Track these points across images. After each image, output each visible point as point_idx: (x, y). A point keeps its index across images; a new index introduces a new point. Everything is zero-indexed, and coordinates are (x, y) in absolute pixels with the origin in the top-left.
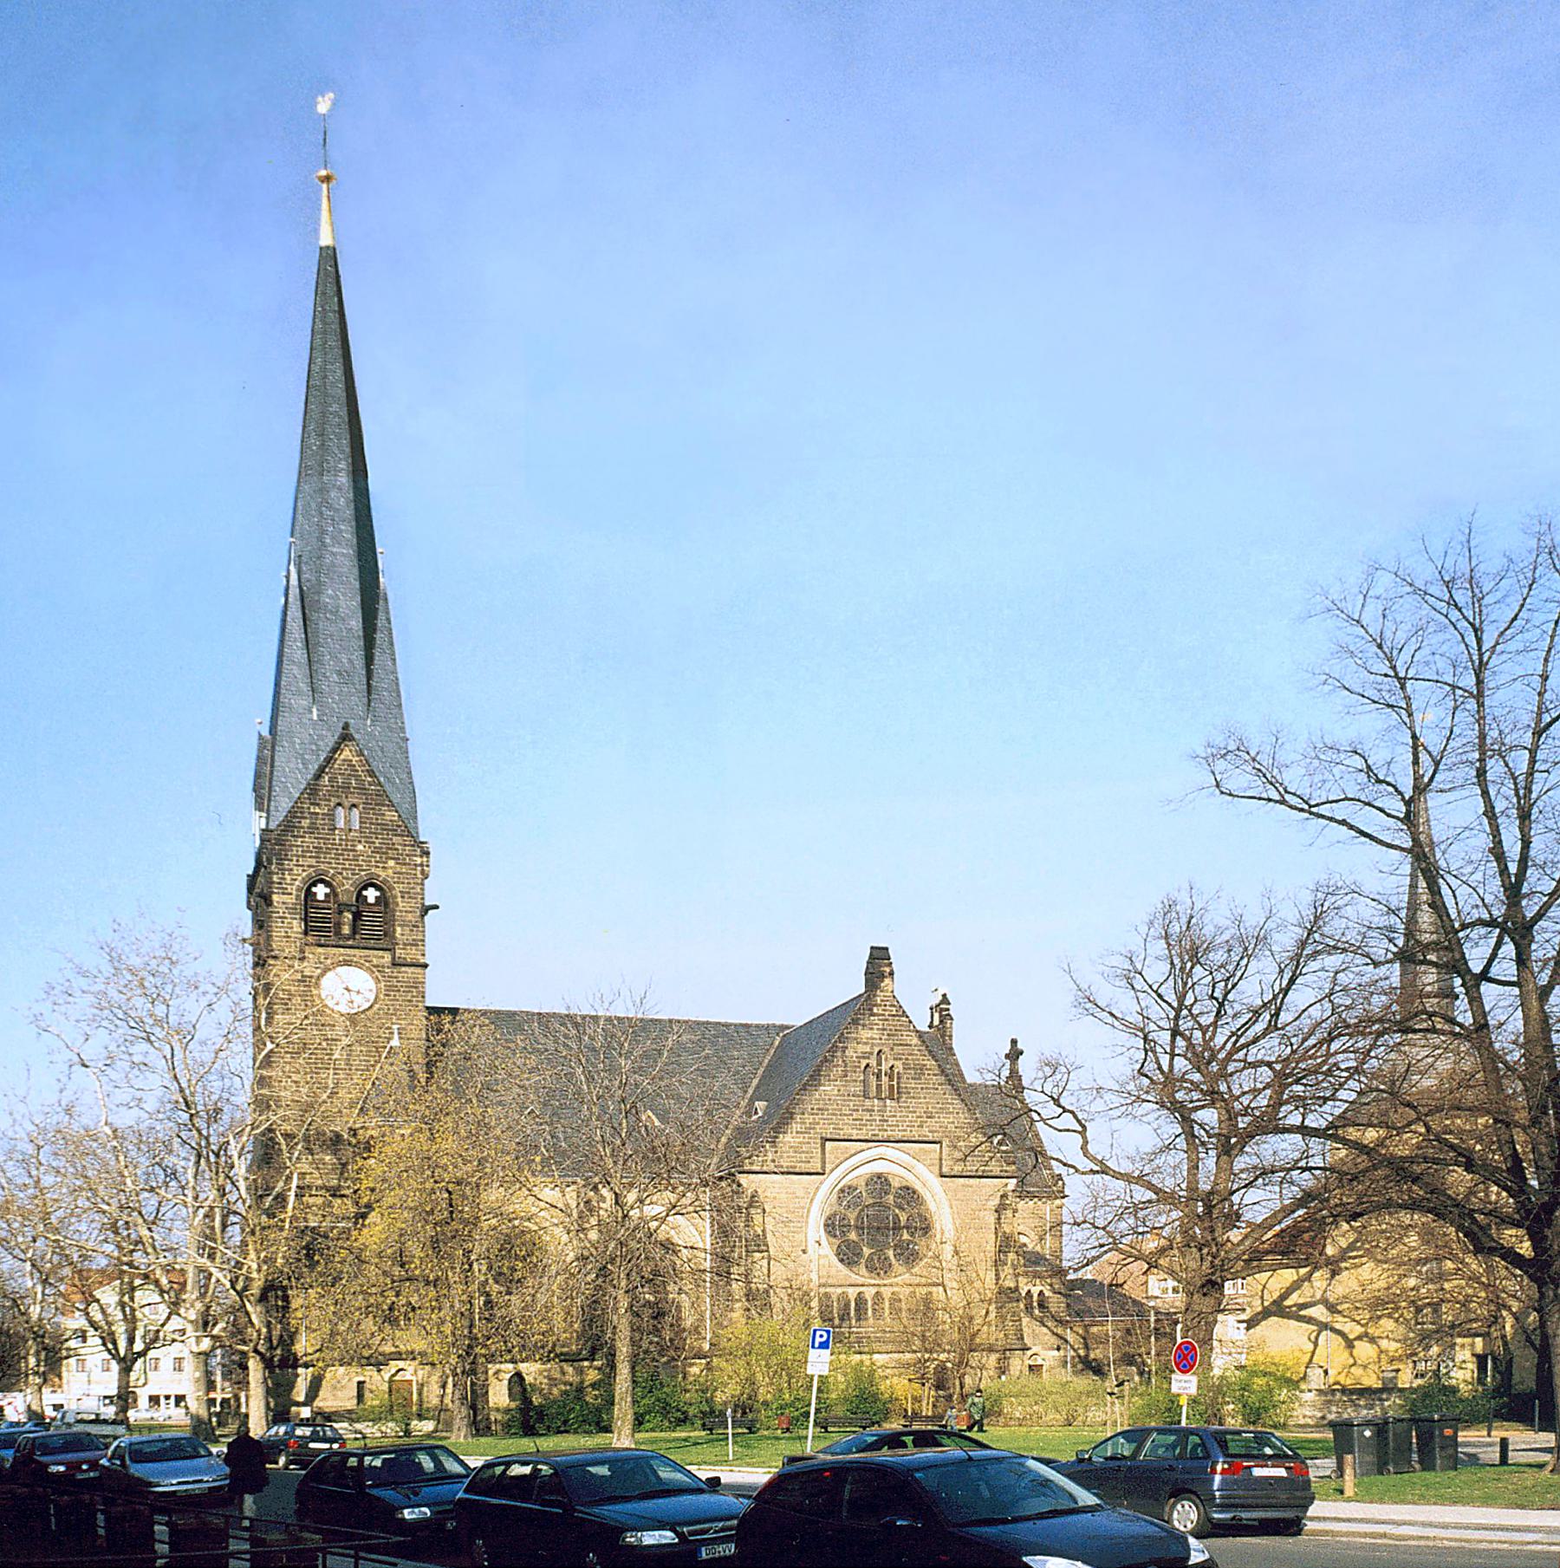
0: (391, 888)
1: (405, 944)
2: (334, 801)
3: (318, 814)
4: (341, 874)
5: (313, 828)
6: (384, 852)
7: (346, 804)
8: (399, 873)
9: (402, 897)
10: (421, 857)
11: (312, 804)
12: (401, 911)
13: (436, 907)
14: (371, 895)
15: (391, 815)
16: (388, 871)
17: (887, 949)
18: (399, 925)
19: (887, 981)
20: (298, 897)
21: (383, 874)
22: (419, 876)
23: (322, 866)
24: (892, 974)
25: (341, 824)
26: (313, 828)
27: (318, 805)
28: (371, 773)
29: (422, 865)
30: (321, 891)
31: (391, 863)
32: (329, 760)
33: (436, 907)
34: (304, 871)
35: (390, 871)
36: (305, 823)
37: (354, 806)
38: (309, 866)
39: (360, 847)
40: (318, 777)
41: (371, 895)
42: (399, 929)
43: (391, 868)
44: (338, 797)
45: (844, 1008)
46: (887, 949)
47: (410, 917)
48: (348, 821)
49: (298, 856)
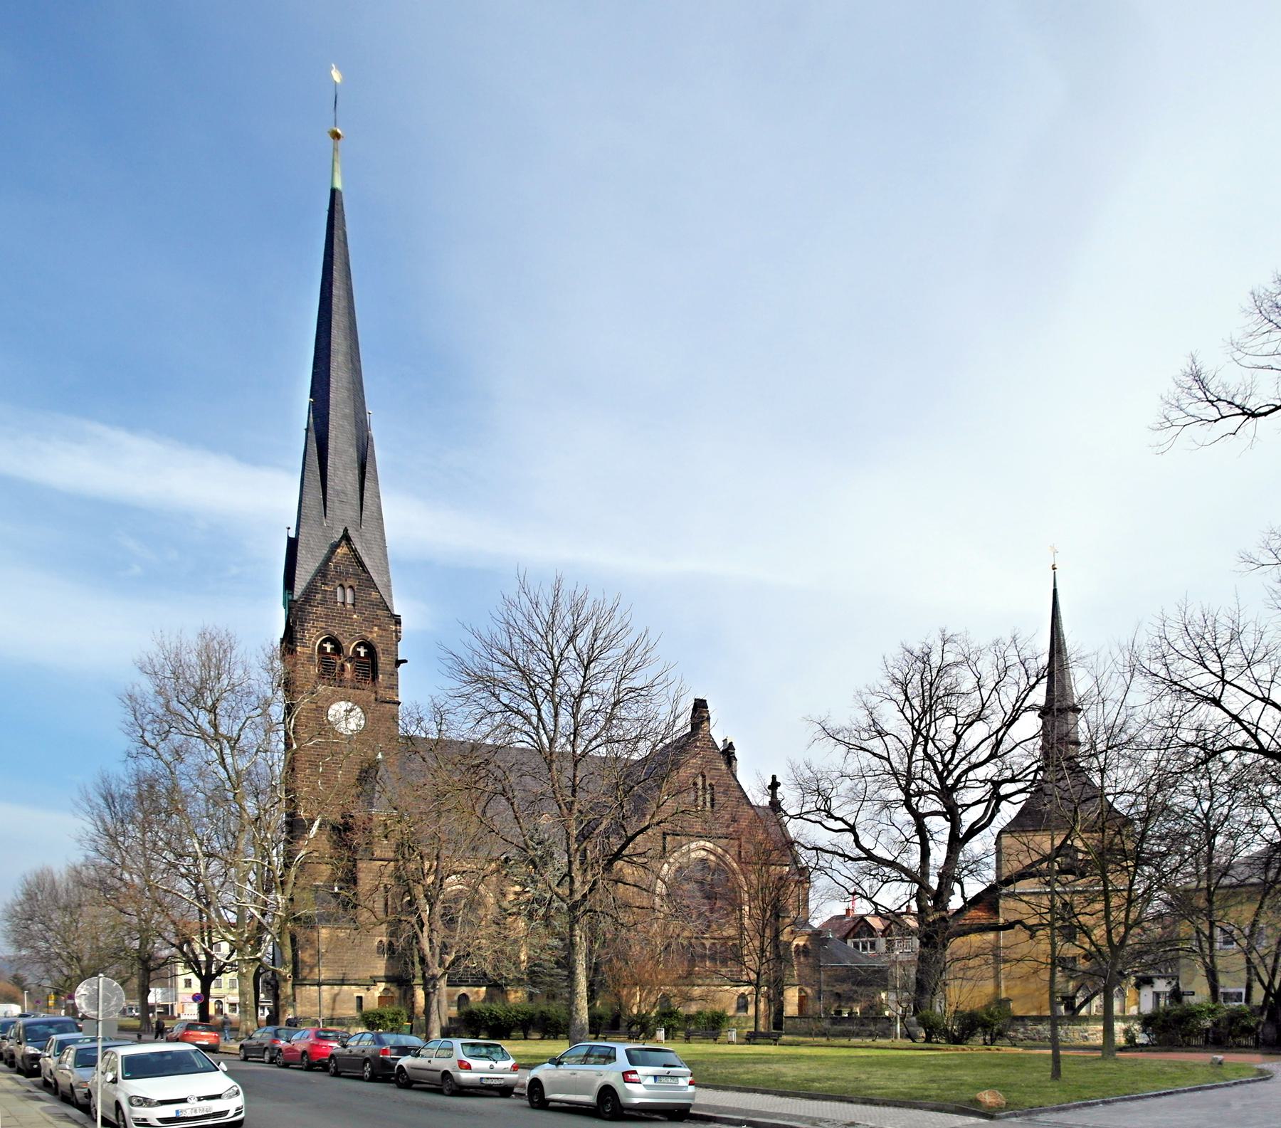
2: (338, 582)
4: (342, 634)
6: (371, 621)
8: (381, 636)
9: (383, 653)
10: (396, 625)
11: (323, 584)
12: (382, 663)
13: (405, 661)
16: (374, 635)
17: (705, 701)
18: (382, 674)
19: (706, 724)
22: (394, 639)
23: (330, 629)
24: (708, 719)
26: (323, 602)
27: (326, 584)
28: (362, 564)
31: (376, 629)
33: (405, 661)
34: (317, 631)
35: (375, 635)
36: (319, 597)
38: (322, 628)
39: (355, 616)
42: (381, 676)
43: (376, 632)
44: (340, 579)
46: (705, 701)
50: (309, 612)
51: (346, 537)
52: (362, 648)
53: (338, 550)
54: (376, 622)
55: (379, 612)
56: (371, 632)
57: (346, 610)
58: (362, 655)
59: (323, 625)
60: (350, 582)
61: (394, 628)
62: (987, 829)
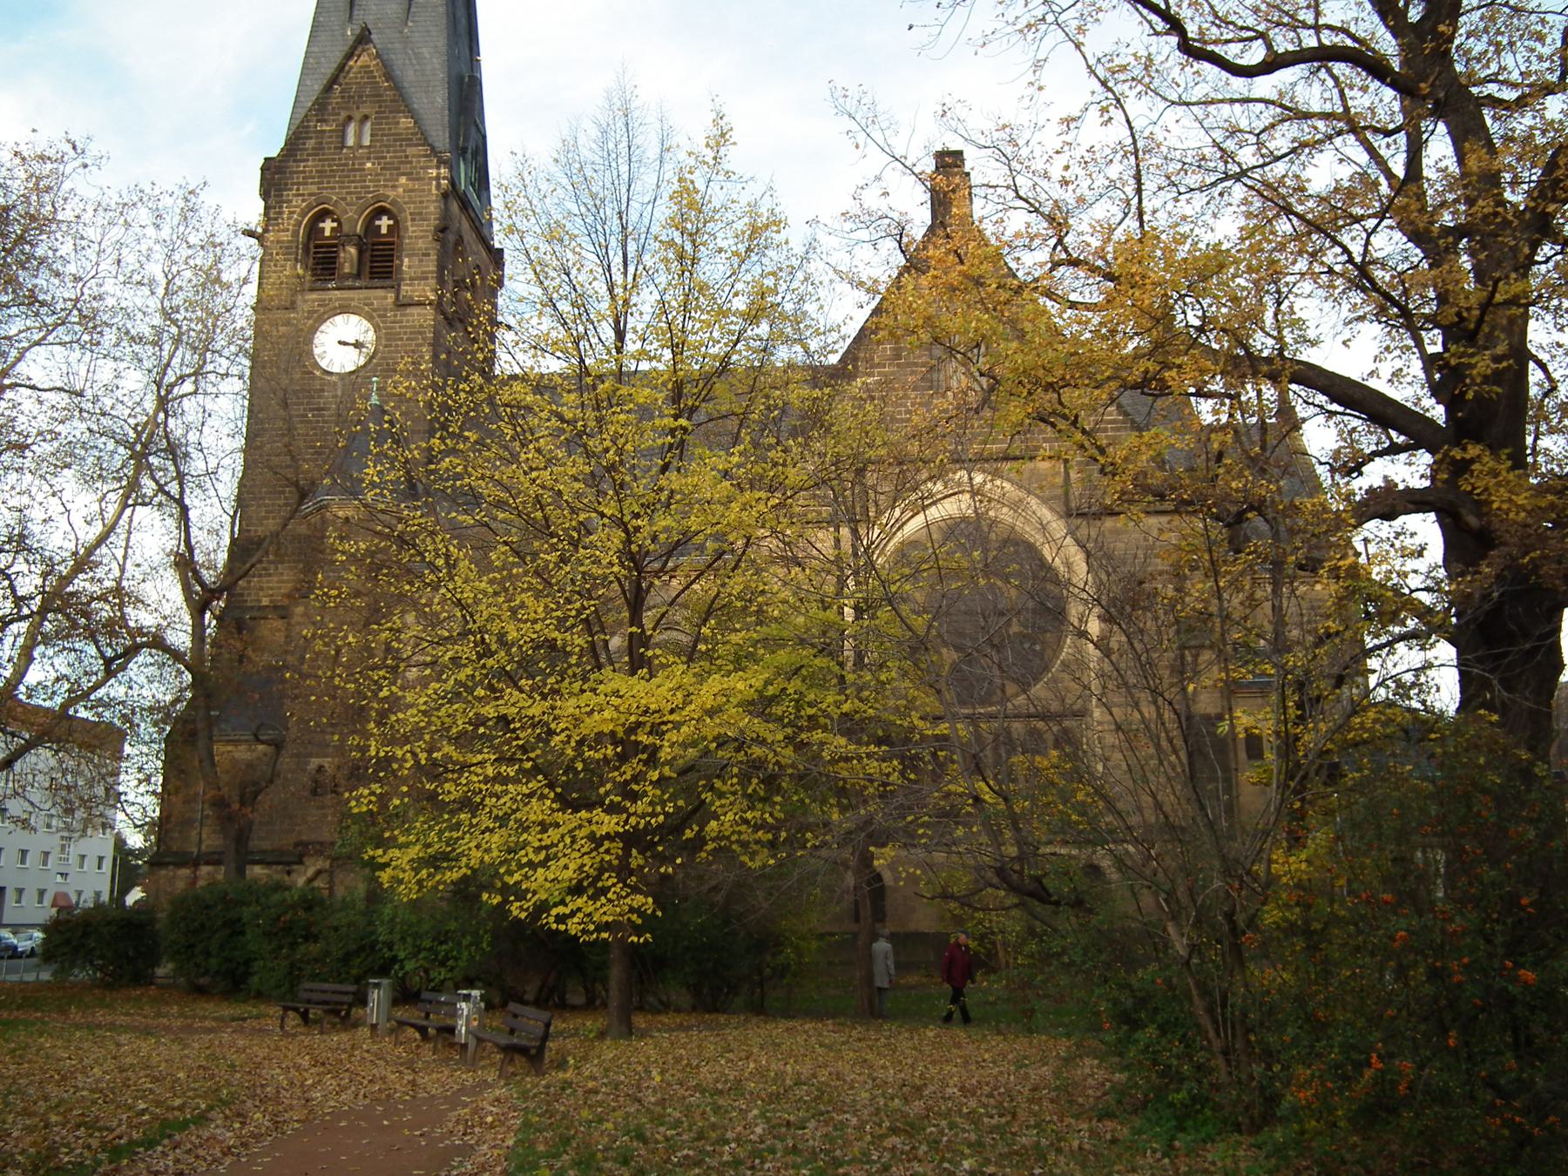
1: (412, 279)
2: (344, 114)
4: (344, 199)
5: (319, 148)
6: (394, 170)
7: (357, 115)
10: (438, 168)
14: (384, 223)
15: (405, 122)
18: (408, 256)
20: (296, 234)
21: (391, 194)
22: (434, 191)
25: (350, 141)
28: (389, 76)
29: (438, 178)
30: (328, 226)
31: (403, 180)
32: (342, 68)
36: (310, 144)
37: (366, 117)
39: (369, 165)
40: (328, 89)
45: (433, 102)
47: (421, 244)
48: (359, 136)
50: (292, 173)
51: (363, 38)
52: (385, 218)
54: (406, 168)
55: (411, 151)
57: (355, 158)
58: (384, 231)
59: (314, 189)
60: (365, 110)
61: (434, 172)
62: (1225, 74)
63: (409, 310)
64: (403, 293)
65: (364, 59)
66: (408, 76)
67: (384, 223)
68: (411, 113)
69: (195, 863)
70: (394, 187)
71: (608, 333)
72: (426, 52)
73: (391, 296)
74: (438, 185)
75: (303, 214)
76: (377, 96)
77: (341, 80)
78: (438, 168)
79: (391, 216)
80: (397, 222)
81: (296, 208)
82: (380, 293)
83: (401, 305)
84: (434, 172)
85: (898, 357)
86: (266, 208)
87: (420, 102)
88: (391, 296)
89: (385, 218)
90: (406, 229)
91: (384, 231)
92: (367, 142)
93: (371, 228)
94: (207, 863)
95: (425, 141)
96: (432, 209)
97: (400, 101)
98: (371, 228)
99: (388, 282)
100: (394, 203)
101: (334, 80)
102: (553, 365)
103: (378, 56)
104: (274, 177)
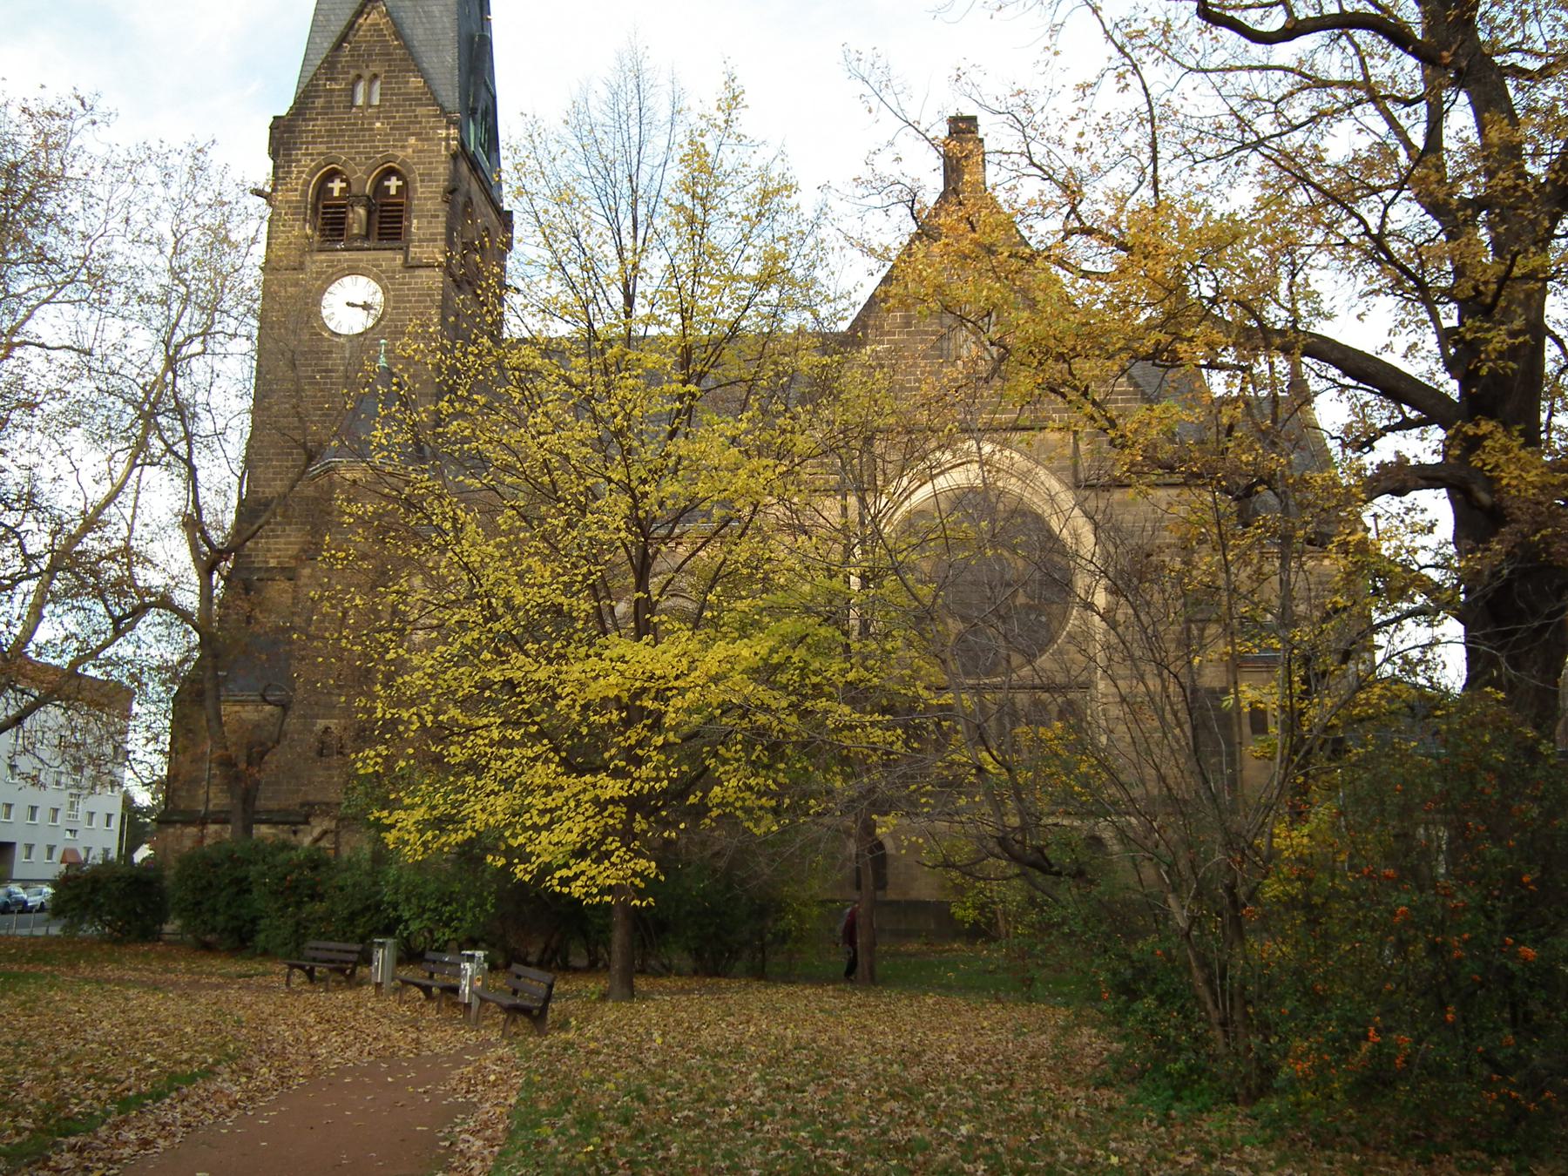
0: (411, 171)
2: (353, 73)
3: (332, 90)
5: (328, 108)
6: (402, 129)
7: (367, 74)
10: (448, 128)
15: (415, 82)
16: (408, 150)
18: (416, 217)
20: (305, 194)
21: (401, 154)
25: (360, 101)
28: (398, 34)
29: (447, 139)
30: (337, 186)
31: (412, 140)
32: (351, 25)
35: (410, 150)
36: (319, 102)
37: (375, 76)
39: (378, 125)
40: (338, 47)
41: (393, 184)
44: (357, 67)
45: (443, 62)
48: (368, 95)
49: (308, 143)
50: (301, 132)
52: (394, 179)
53: (361, 21)
54: (413, 128)
55: (420, 111)
56: (403, 147)
58: (393, 191)
59: (322, 148)
60: (375, 69)
61: (443, 133)
62: (1244, 41)
63: (418, 272)
64: (411, 255)
65: (374, 16)
66: (418, 33)
67: (393, 184)
68: (421, 72)
69: (203, 822)
70: (403, 147)
71: (617, 298)
72: (436, 10)
73: (399, 258)
74: (448, 147)
75: (312, 174)
76: (387, 54)
77: (351, 38)
78: (448, 128)
79: (400, 176)
80: (406, 183)
81: (305, 166)
82: (389, 254)
83: (409, 267)
84: (443, 133)
85: (908, 324)
86: (275, 167)
87: (430, 61)
88: (399, 258)
89: (394, 179)
90: (415, 190)
91: (393, 191)
92: (376, 101)
93: (380, 188)
94: (214, 822)
95: (435, 101)
96: (441, 170)
97: (410, 60)
98: (380, 188)
99: (397, 244)
100: (403, 163)
101: (343, 38)
102: (561, 329)
103: (388, 14)
104: (283, 136)
